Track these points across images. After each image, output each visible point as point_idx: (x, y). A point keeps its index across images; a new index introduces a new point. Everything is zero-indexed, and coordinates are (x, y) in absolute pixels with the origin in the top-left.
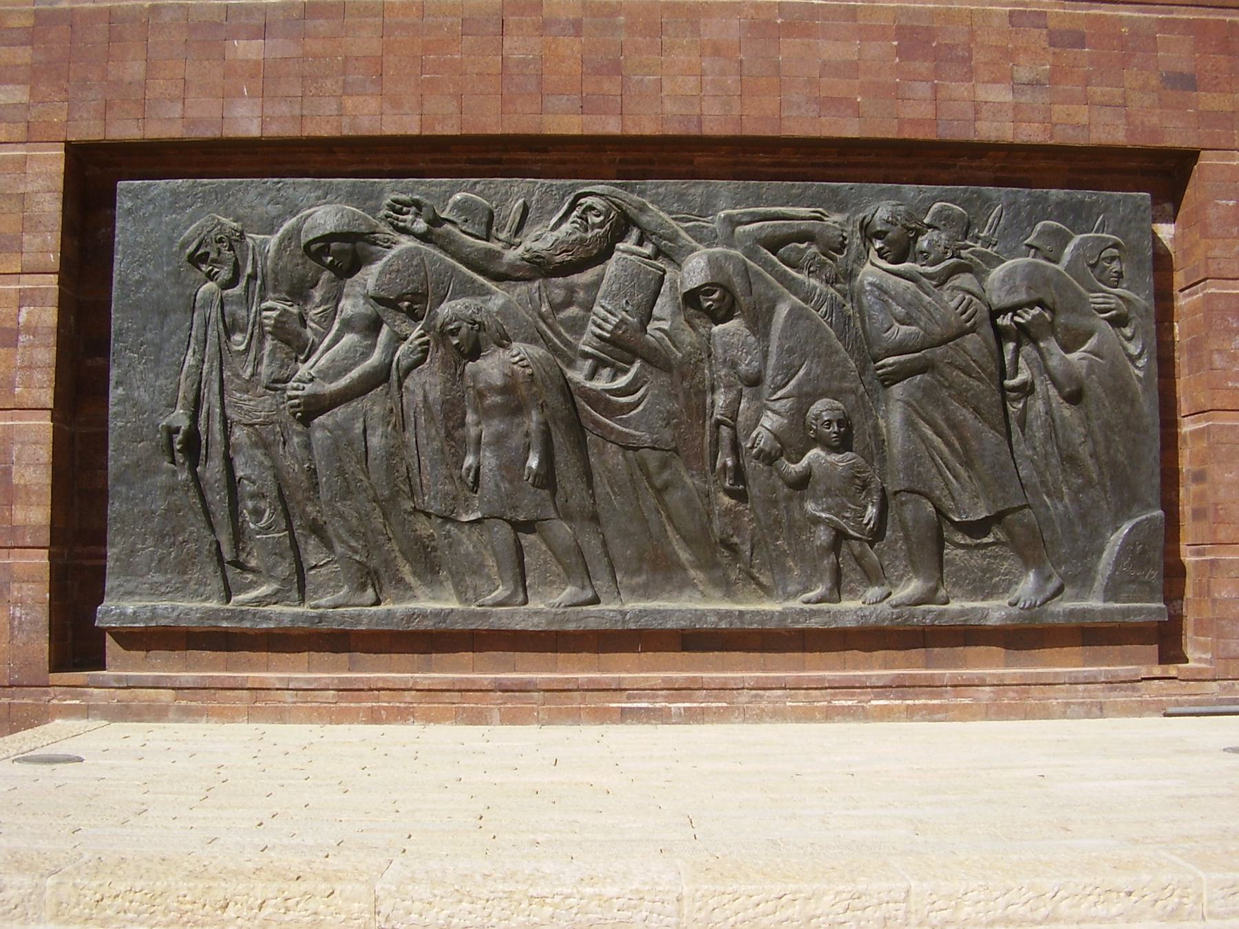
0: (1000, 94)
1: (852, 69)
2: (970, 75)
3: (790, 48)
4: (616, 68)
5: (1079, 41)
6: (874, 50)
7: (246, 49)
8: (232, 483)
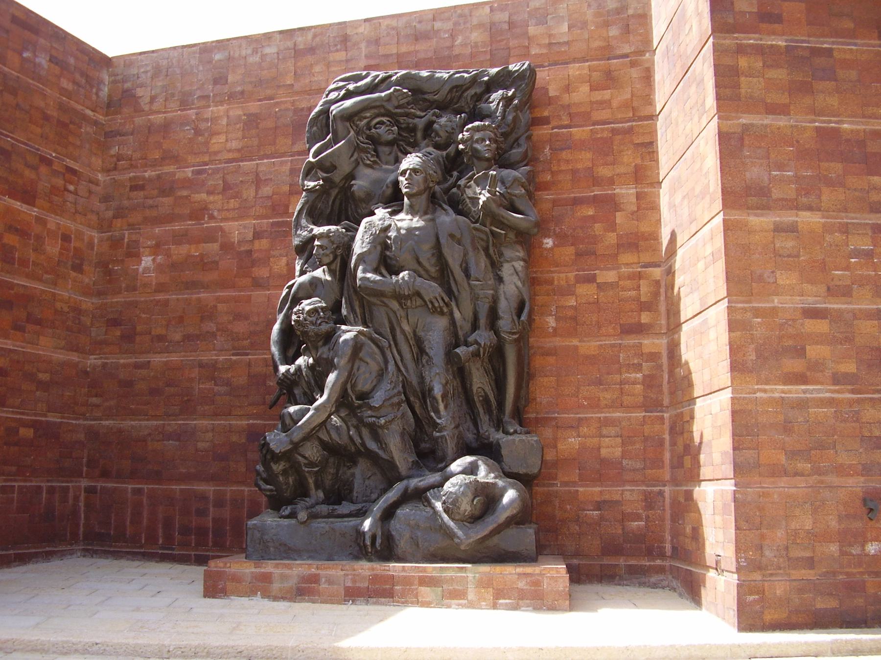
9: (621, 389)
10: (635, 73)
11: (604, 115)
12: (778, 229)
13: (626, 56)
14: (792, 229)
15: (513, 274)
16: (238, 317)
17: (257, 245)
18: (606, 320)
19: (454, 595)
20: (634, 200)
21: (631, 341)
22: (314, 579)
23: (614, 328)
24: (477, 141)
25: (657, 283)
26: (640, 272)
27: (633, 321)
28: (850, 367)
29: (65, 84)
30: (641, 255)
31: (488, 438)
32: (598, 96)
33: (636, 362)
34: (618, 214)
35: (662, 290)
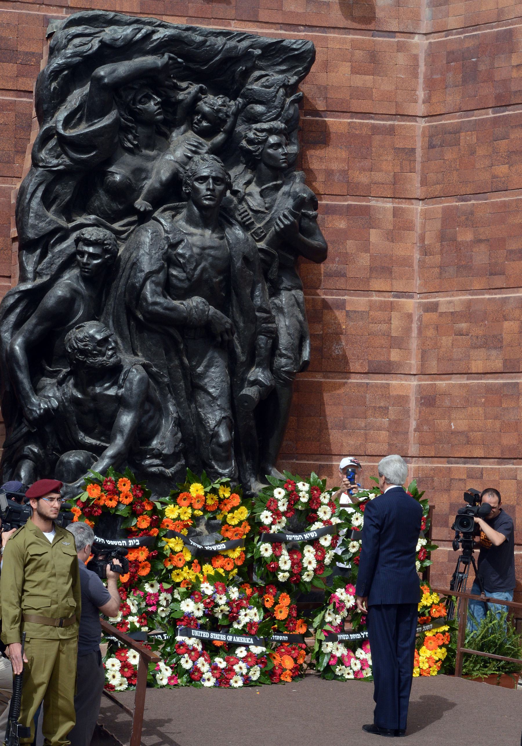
9: (366, 434)
10: (401, 59)
11: (364, 106)
13: (392, 33)
15: (293, 306)
18: (353, 354)
20: (390, 217)
21: (378, 380)
23: (362, 365)
24: (272, 146)
25: (410, 316)
26: (392, 302)
27: (382, 358)
30: (394, 282)
31: (250, 489)
32: (359, 81)
33: (382, 404)
34: (373, 231)
35: (415, 326)
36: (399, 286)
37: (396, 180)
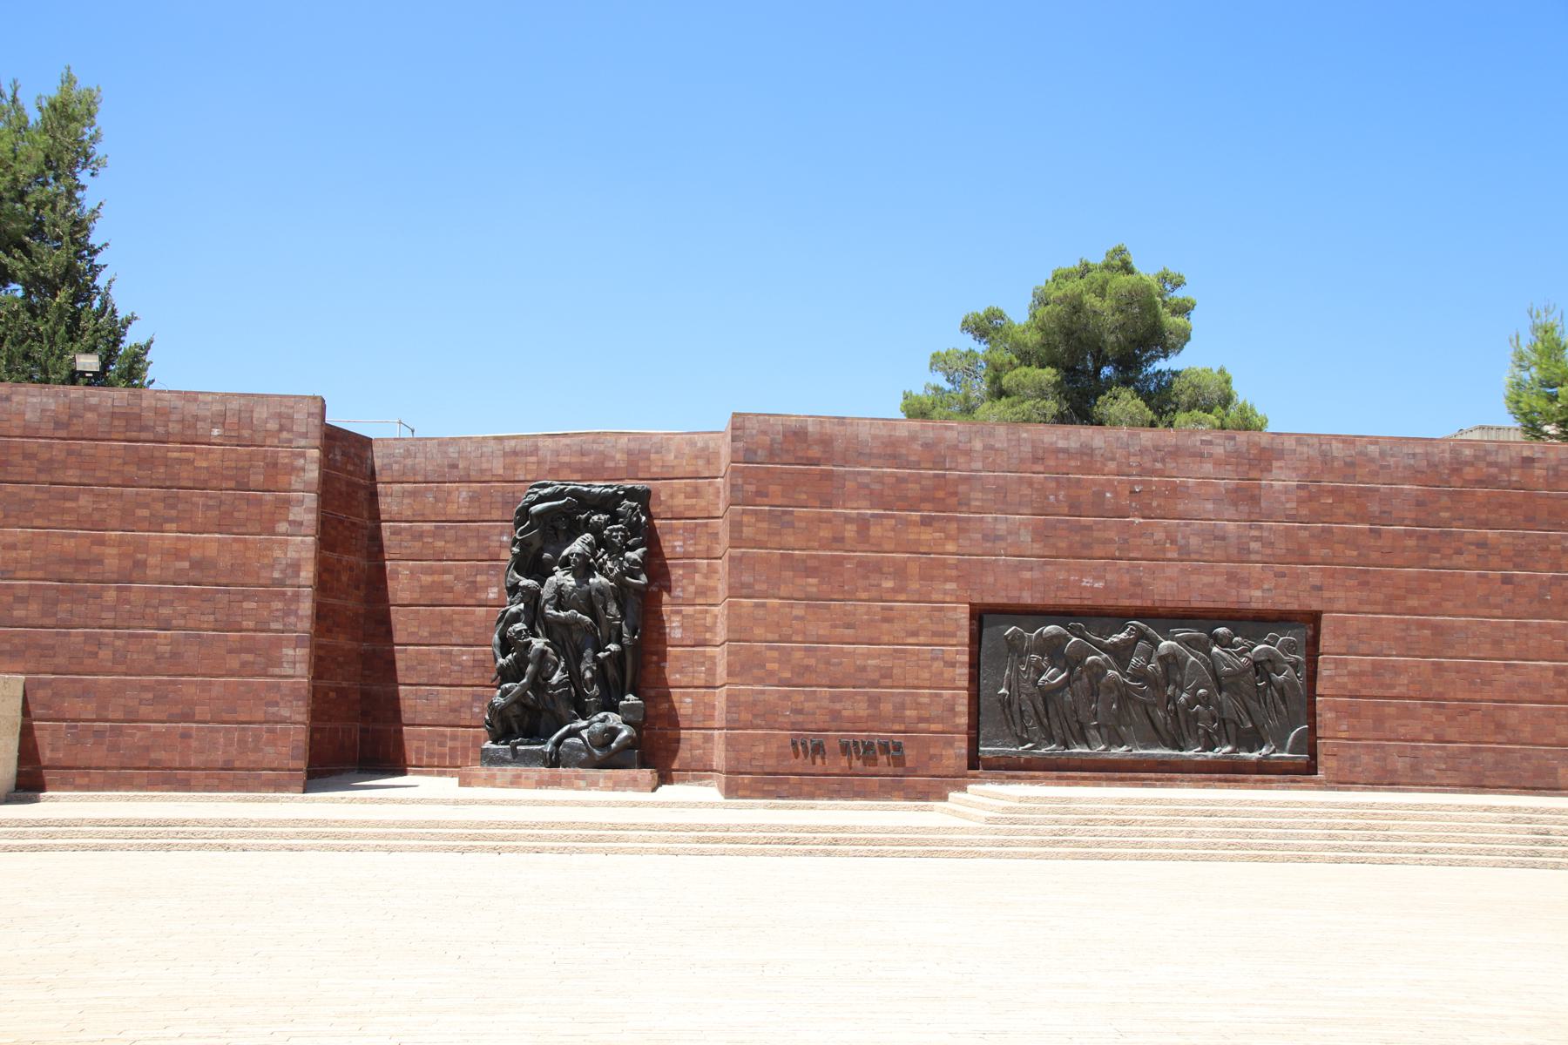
0: (1258, 593)
1: (1212, 585)
2: (1249, 587)
3: (1194, 578)
4: (1140, 584)
5: (1283, 575)
6: (1218, 579)
7: (1027, 575)
8: (1021, 712)
10: (711, 490)
12: (757, 605)
14: (764, 605)
16: (467, 624)
17: (479, 578)
19: (593, 784)
22: (519, 776)
28: (787, 675)
29: (350, 468)
32: (688, 502)
36: (710, 601)
37: (709, 549)
